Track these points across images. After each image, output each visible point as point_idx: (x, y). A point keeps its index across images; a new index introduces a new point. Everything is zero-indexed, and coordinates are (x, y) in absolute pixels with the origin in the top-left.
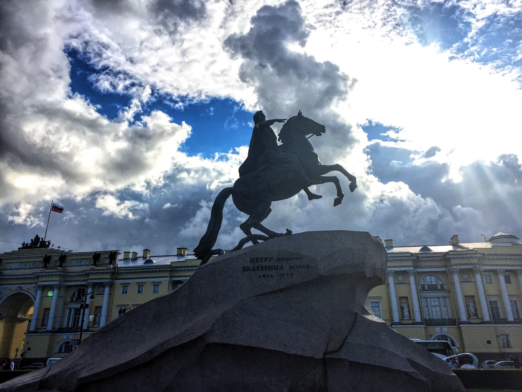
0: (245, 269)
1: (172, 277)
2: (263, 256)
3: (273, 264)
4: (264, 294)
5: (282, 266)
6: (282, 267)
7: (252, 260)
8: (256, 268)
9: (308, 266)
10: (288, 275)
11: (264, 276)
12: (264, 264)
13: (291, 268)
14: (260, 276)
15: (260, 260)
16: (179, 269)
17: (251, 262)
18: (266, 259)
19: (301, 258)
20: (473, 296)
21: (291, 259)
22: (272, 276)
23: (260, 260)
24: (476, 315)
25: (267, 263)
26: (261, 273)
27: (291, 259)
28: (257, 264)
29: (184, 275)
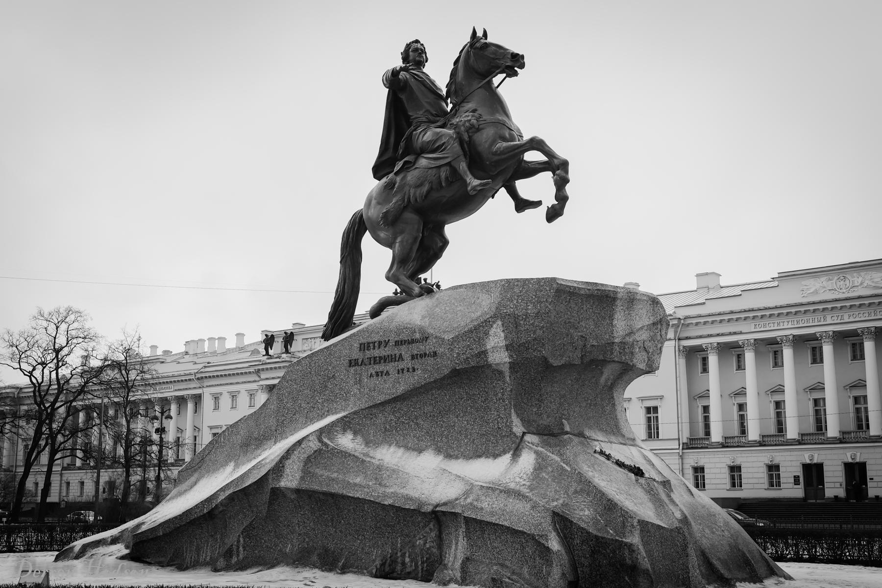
0: (353, 363)
1: (679, 339)
2: (376, 338)
3: (389, 353)
4: (375, 406)
6: (401, 358)
7: (364, 347)
8: (366, 361)
9: (435, 353)
10: (408, 371)
11: (377, 374)
12: (377, 353)
13: (413, 357)
16: (694, 321)
17: (360, 350)
18: (380, 343)
21: (413, 341)
22: (387, 373)
27: (413, 341)
28: (369, 354)
29: (705, 333)
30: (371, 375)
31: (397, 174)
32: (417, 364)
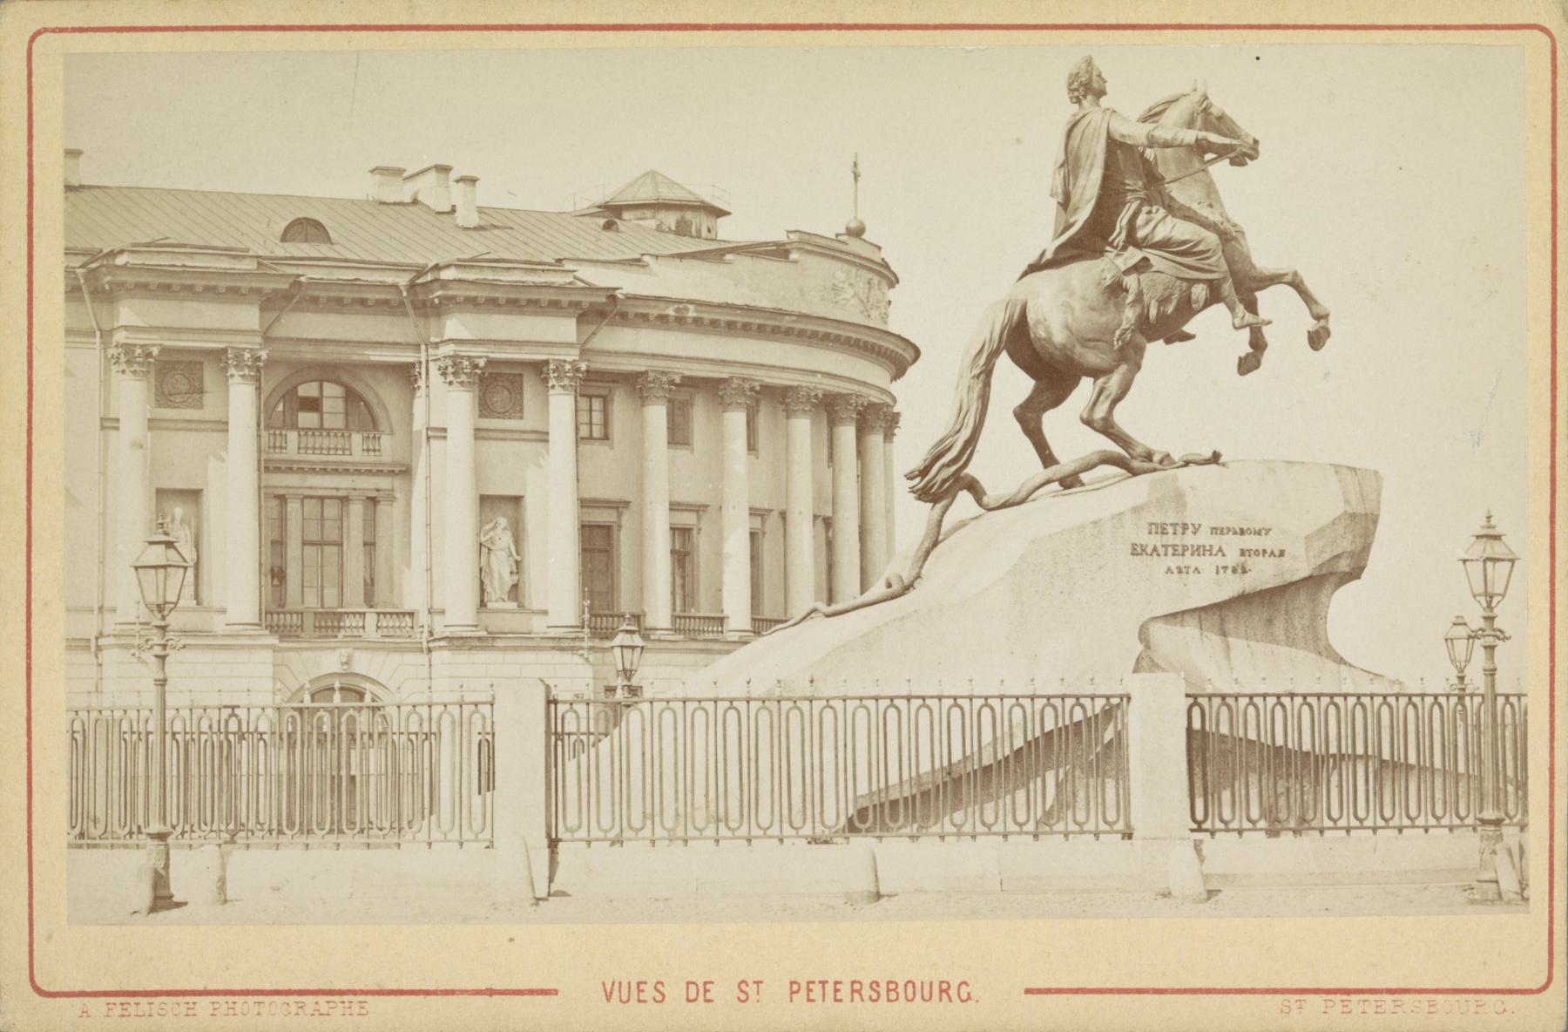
0: (1137, 550)
5: (1220, 550)
8: (1161, 550)
12: (1177, 540)
13: (1243, 553)
14: (1169, 570)
15: (1170, 530)
19: (1268, 531)
20: (517, 500)
21: (1242, 532)
23: (1170, 530)
24: (515, 591)
25: (1190, 539)
26: (1173, 562)
30: (1169, 570)
31: (1127, 272)
32: (1251, 562)
